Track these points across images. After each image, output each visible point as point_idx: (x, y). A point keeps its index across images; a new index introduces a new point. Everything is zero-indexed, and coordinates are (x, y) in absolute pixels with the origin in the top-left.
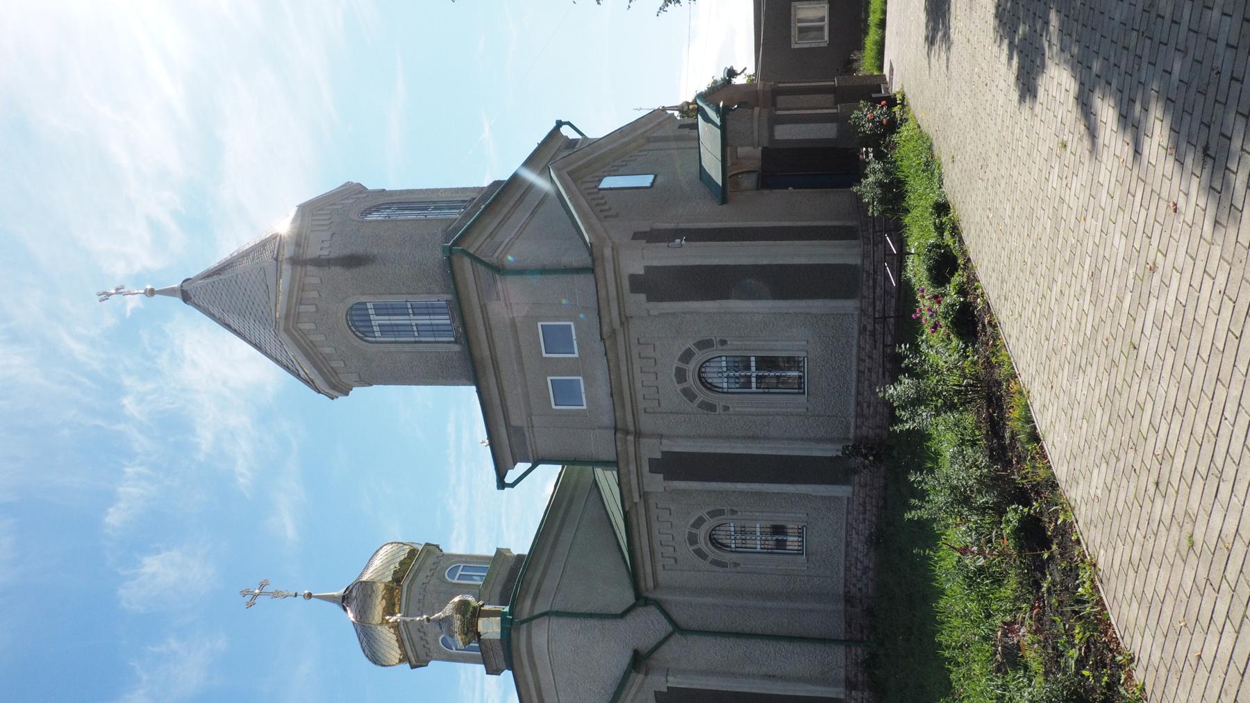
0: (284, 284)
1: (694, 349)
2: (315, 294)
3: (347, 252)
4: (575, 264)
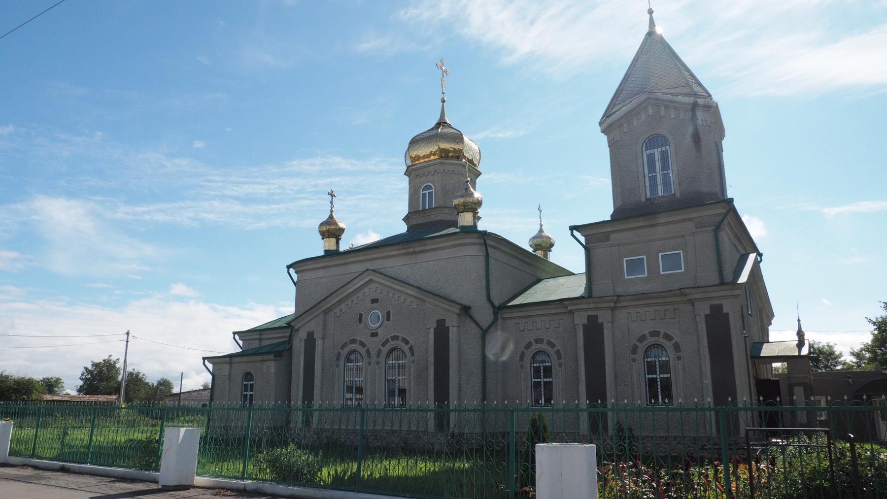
1: (673, 342)
3: (701, 136)
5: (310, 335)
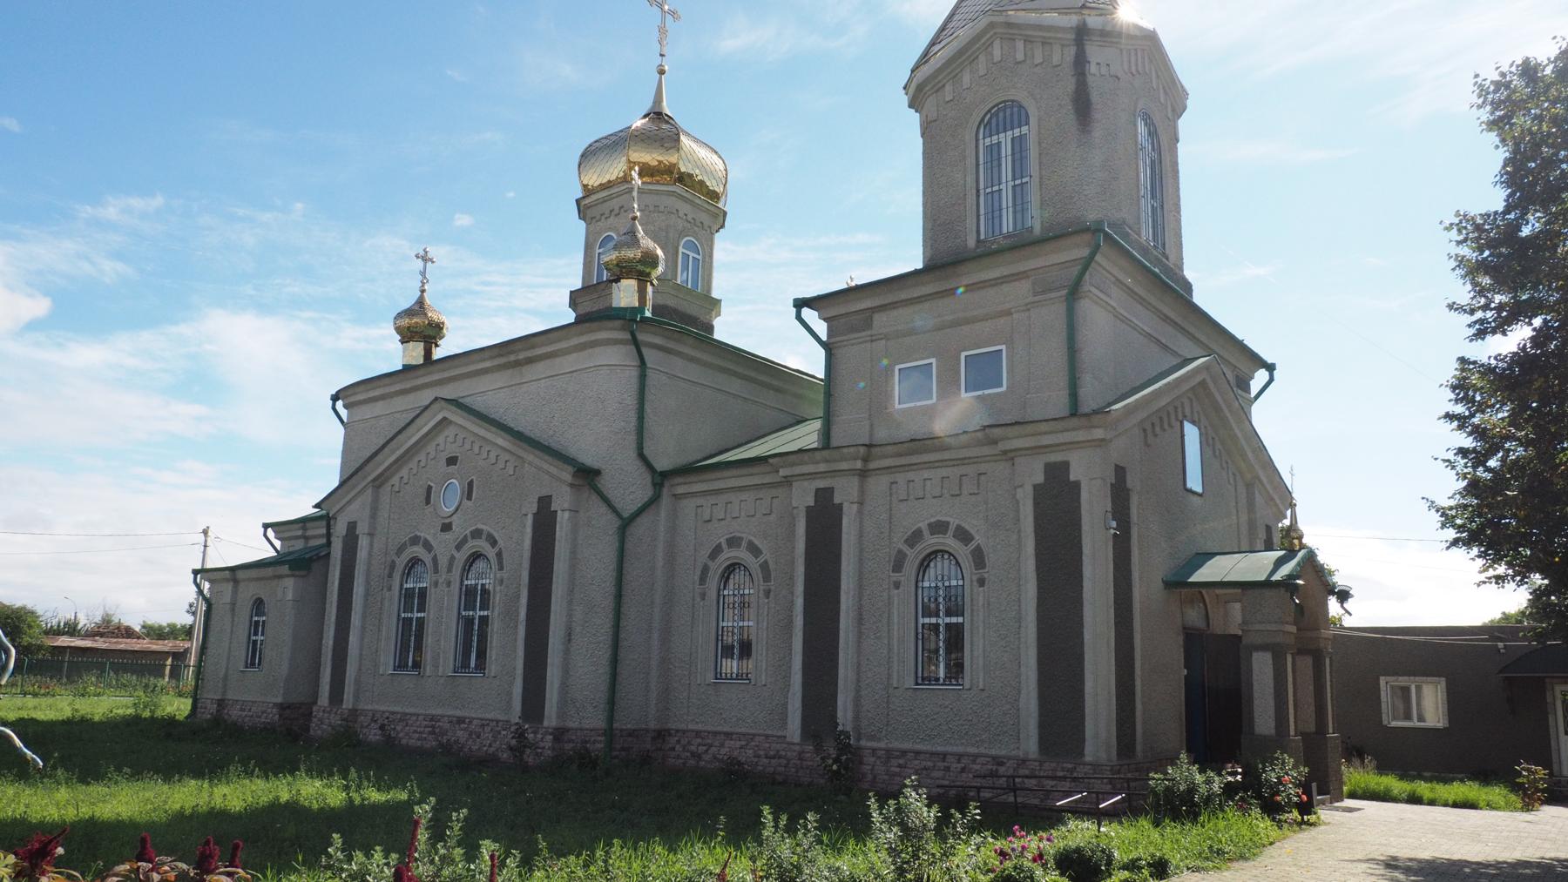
0: (1052, 18)
1: (972, 545)
2: (1038, 60)
3: (1095, 97)
4: (1082, 392)
5: (352, 527)
